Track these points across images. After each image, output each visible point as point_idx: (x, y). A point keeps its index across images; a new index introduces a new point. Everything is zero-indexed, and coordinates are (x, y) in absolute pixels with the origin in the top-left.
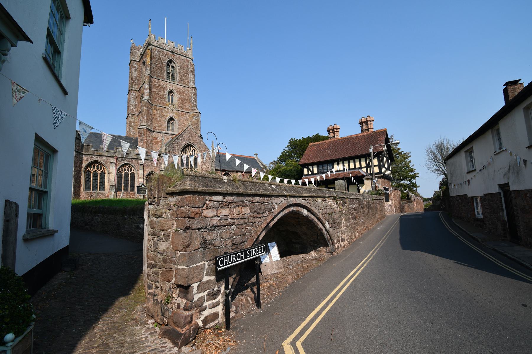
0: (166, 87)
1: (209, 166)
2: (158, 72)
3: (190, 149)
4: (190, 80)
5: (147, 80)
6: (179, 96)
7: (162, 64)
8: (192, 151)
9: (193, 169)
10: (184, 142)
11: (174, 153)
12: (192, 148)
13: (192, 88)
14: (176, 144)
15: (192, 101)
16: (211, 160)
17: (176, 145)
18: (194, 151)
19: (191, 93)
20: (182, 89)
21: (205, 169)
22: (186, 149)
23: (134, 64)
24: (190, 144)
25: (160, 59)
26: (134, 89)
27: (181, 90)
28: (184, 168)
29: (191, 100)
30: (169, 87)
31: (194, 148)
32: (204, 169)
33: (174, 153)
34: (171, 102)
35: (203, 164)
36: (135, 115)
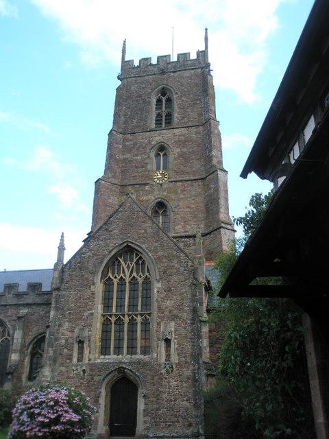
1: (182, 299)
3: (131, 260)
8: (137, 263)
9: (136, 315)
10: (111, 245)
11: (82, 276)
12: (137, 255)
14: (88, 254)
16: (189, 281)
17: (89, 256)
18: (140, 262)
21: (170, 312)
22: (119, 262)
24: (128, 246)
28: (111, 316)
31: (140, 255)
32: (167, 313)
33: (82, 276)
35: (162, 296)
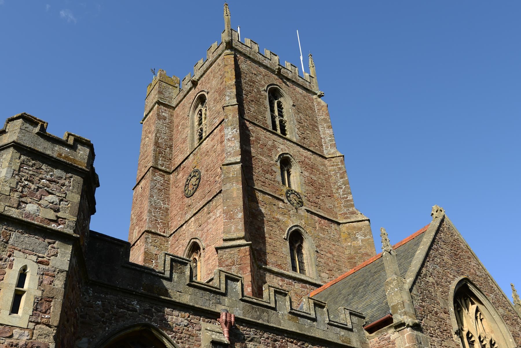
0: (274, 147)
2: (252, 109)
4: (323, 140)
5: (230, 118)
6: (306, 174)
7: (259, 92)
13: (333, 159)
15: (341, 191)
19: (334, 170)
20: (310, 159)
23: (162, 112)
25: (254, 82)
26: (160, 167)
27: (307, 160)
29: (337, 189)
30: (282, 146)
34: (287, 186)
36: (160, 235)
